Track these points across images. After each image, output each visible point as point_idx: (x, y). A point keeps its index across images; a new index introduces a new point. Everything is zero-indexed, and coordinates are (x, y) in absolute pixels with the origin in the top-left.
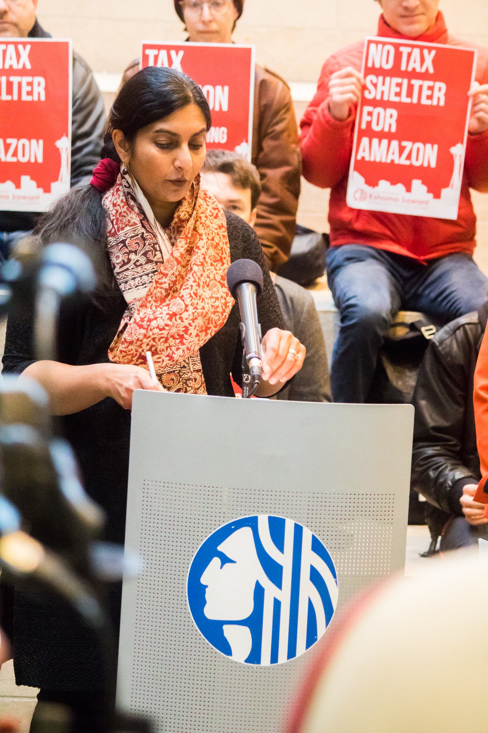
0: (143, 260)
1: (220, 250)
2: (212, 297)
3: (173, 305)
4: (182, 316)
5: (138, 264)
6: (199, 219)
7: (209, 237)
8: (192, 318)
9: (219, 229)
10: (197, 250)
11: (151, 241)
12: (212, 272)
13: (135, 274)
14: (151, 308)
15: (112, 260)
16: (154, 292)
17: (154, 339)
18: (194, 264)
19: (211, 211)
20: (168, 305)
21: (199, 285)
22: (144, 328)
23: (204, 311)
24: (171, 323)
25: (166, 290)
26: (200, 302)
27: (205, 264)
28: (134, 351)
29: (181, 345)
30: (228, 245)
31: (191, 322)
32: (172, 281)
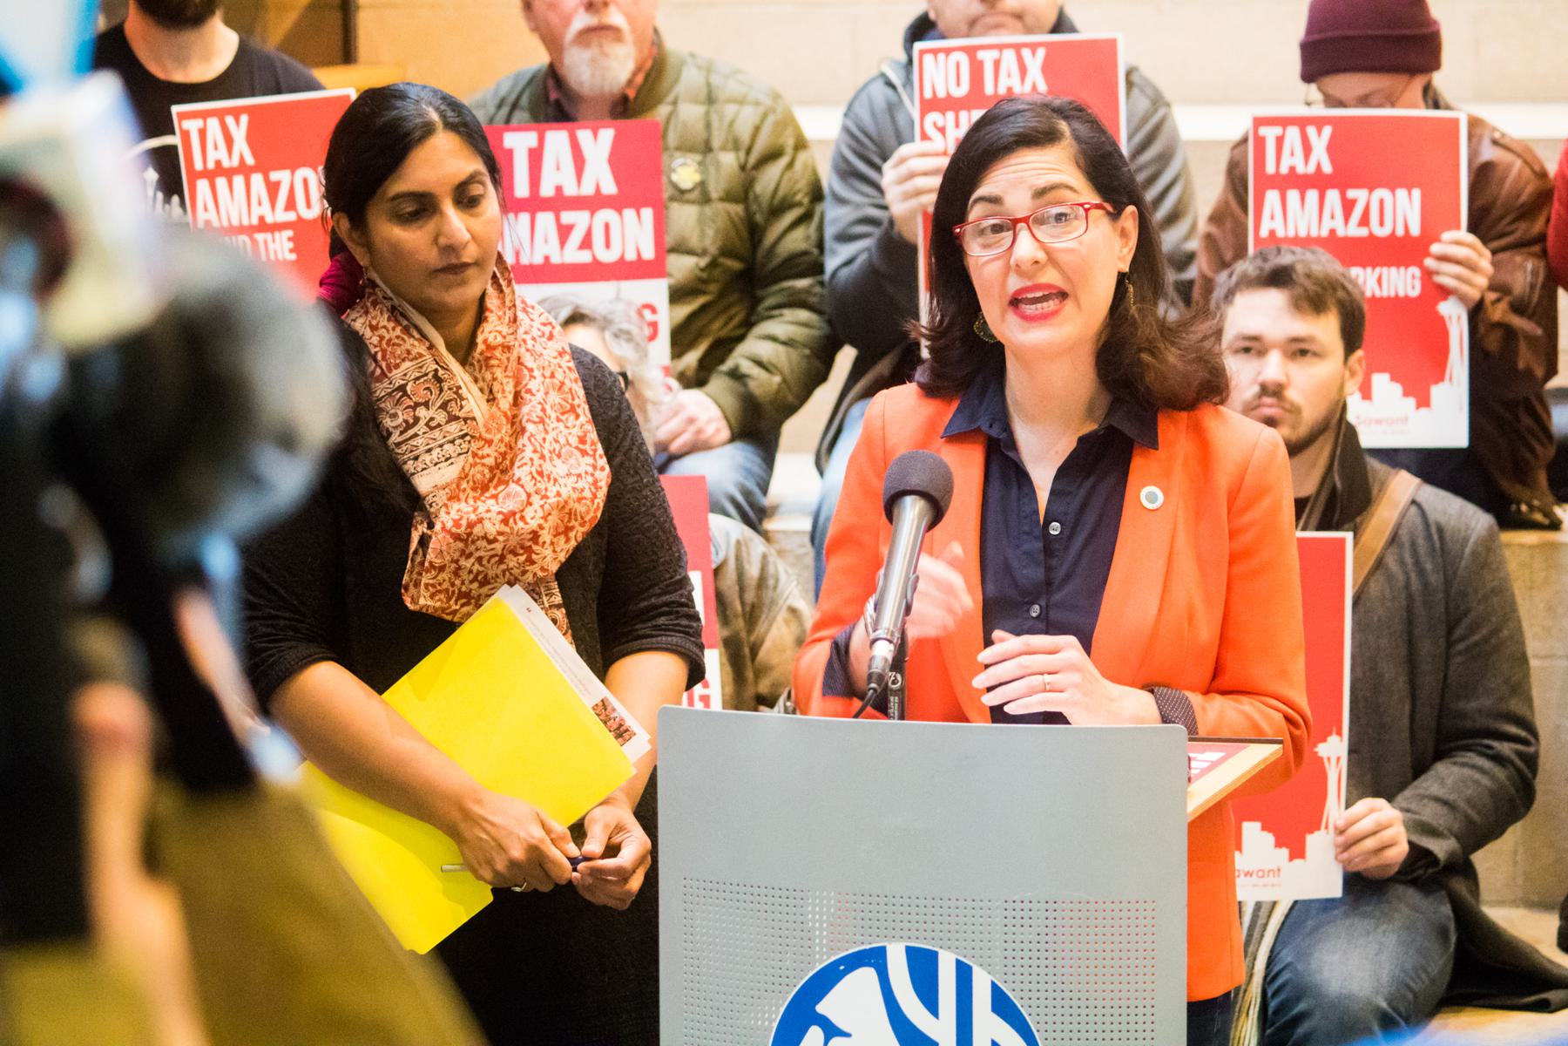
0: (441, 417)
3: (504, 498)
4: (524, 514)
5: (433, 424)
6: (522, 343)
7: (545, 372)
8: (542, 515)
9: (559, 358)
10: (528, 396)
11: (452, 382)
12: (561, 432)
13: (430, 442)
14: (466, 501)
15: (381, 422)
16: (471, 473)
17: (480, 559)
18: (528, 420)
19: (539, 330)
21: (543, 457)
22: (461, 540)
23: (560, 499)
24: (507, 530)
25: (491, 469)
26: (549, 486)
28: (446, 585)
30: (580, 384)
31: (542, 521)
32: (501, 454)
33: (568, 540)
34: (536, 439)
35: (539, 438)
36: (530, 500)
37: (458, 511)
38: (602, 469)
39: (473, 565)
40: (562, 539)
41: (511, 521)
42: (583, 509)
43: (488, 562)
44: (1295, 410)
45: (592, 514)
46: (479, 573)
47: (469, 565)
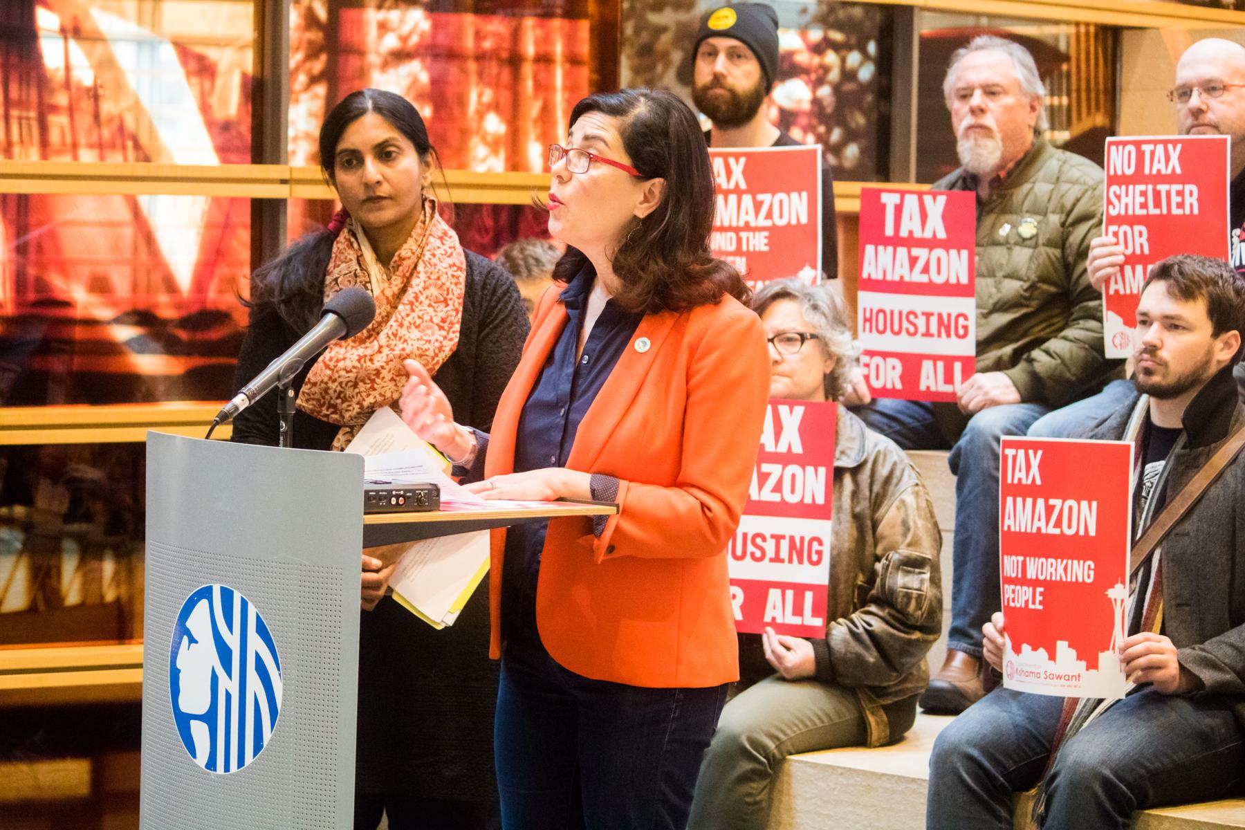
14: (346, 348)
19: (445, 250)
20: (366, 348)
22: (330, 369)
23: (404, 353)
24: (359, 365)
31: (384, 364)
35: (403, 314)
38: (451, 340)
41: (363, 360)
43: (346, 385)
44: (1165, 364)
46: (340, 393)
47: (334, 387)
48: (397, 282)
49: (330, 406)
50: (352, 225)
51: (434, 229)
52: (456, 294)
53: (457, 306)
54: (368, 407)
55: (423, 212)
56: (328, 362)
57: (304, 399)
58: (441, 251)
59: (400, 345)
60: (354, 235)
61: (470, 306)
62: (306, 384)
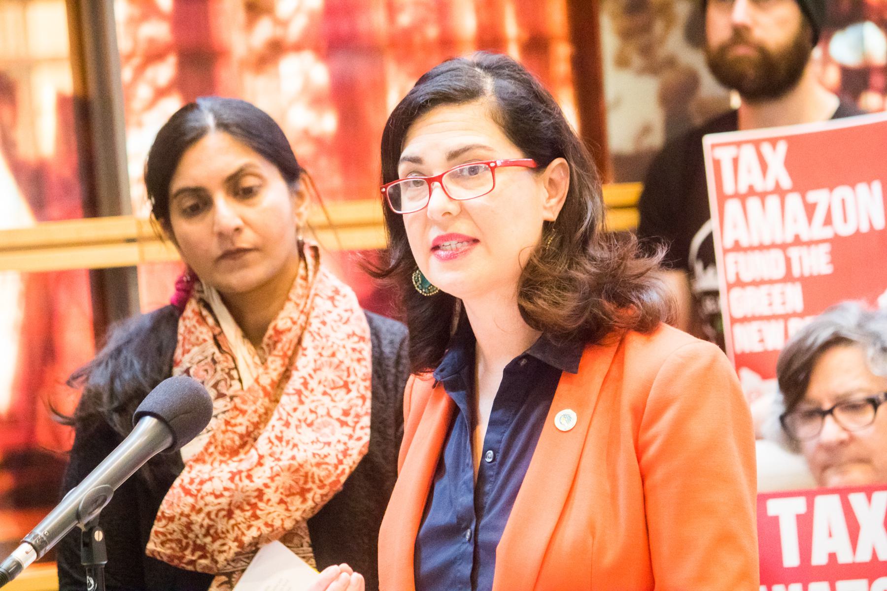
1: (343, 371)
2: (318, 441)
4: (251, 473)
12: (323, 405)
14: (212, 464)
19: (339, 315)
20: (241, 460)
21: (287, 424)
22: (191, 495)
24: (232, 486)
25: (241, 436)
27: (306, 393)
28: (176, 536)
29: (253, 521)
31: (268, 481)
33: (304, 500)
34: (284, 409)
35: (289, 408)
36: (262, 461)
37: (200, 471)
38: (359, 439)
39: (204, 519)
40: (297, 500)
41: (237, 478)
42: (323, 473)
43: (217, 515)
45: (333, 478)
46: (209, 527)
48: (276, 365)
49: (197, 547)
50: (202, 292)
51: (320, 286)
52: (360, 374)
53: (363, 391)
54: (250, 544)
55: (302, 264)
56: (188, 486)
57: (158, 541)
58: (334, 316)
59: (288, 453)
60: (208, 307)
61: (381, 391)
62: (160, 520)
